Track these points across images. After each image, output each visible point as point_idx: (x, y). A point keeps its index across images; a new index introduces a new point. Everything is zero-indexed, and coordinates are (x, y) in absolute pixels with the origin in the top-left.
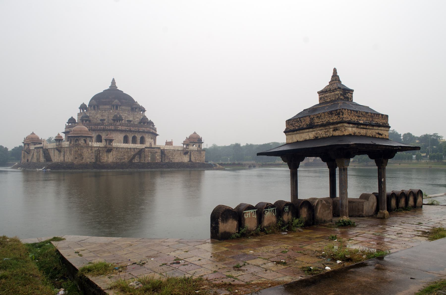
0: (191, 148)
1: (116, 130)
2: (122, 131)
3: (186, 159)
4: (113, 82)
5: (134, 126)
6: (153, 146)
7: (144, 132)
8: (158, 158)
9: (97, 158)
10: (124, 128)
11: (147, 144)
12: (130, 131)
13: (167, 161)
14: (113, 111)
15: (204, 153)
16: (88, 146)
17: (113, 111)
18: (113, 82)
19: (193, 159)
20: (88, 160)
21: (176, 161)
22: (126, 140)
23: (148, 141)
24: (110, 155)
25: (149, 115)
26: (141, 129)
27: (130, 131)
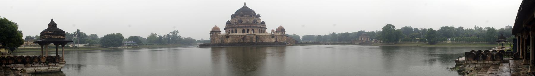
0: (277, 34)
1: (238, 27)
2: (241, 27)
3: (273, 40)
4: (245, 4)
5: (250, 24)
6: (252, 34)
7: (253, 27)
8: (254, 40)
9: (222, 41)
10: (242, 26)
11: (249, 33)
12: (246, 27)
13: (260, 41)
14: (245, 17)
15: (285, 37)
16: (217, 36)
17: (245, 17)
18: (245, 4)
19: (278, 40)
20: (218, 42)
21: (267, 41)
22: (244, 31)
23: (251, 32)
24: (229, 39)
25: (262, 19)
26: (252, 26)
27: (246, 27)
